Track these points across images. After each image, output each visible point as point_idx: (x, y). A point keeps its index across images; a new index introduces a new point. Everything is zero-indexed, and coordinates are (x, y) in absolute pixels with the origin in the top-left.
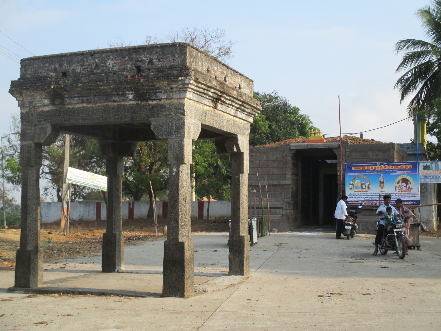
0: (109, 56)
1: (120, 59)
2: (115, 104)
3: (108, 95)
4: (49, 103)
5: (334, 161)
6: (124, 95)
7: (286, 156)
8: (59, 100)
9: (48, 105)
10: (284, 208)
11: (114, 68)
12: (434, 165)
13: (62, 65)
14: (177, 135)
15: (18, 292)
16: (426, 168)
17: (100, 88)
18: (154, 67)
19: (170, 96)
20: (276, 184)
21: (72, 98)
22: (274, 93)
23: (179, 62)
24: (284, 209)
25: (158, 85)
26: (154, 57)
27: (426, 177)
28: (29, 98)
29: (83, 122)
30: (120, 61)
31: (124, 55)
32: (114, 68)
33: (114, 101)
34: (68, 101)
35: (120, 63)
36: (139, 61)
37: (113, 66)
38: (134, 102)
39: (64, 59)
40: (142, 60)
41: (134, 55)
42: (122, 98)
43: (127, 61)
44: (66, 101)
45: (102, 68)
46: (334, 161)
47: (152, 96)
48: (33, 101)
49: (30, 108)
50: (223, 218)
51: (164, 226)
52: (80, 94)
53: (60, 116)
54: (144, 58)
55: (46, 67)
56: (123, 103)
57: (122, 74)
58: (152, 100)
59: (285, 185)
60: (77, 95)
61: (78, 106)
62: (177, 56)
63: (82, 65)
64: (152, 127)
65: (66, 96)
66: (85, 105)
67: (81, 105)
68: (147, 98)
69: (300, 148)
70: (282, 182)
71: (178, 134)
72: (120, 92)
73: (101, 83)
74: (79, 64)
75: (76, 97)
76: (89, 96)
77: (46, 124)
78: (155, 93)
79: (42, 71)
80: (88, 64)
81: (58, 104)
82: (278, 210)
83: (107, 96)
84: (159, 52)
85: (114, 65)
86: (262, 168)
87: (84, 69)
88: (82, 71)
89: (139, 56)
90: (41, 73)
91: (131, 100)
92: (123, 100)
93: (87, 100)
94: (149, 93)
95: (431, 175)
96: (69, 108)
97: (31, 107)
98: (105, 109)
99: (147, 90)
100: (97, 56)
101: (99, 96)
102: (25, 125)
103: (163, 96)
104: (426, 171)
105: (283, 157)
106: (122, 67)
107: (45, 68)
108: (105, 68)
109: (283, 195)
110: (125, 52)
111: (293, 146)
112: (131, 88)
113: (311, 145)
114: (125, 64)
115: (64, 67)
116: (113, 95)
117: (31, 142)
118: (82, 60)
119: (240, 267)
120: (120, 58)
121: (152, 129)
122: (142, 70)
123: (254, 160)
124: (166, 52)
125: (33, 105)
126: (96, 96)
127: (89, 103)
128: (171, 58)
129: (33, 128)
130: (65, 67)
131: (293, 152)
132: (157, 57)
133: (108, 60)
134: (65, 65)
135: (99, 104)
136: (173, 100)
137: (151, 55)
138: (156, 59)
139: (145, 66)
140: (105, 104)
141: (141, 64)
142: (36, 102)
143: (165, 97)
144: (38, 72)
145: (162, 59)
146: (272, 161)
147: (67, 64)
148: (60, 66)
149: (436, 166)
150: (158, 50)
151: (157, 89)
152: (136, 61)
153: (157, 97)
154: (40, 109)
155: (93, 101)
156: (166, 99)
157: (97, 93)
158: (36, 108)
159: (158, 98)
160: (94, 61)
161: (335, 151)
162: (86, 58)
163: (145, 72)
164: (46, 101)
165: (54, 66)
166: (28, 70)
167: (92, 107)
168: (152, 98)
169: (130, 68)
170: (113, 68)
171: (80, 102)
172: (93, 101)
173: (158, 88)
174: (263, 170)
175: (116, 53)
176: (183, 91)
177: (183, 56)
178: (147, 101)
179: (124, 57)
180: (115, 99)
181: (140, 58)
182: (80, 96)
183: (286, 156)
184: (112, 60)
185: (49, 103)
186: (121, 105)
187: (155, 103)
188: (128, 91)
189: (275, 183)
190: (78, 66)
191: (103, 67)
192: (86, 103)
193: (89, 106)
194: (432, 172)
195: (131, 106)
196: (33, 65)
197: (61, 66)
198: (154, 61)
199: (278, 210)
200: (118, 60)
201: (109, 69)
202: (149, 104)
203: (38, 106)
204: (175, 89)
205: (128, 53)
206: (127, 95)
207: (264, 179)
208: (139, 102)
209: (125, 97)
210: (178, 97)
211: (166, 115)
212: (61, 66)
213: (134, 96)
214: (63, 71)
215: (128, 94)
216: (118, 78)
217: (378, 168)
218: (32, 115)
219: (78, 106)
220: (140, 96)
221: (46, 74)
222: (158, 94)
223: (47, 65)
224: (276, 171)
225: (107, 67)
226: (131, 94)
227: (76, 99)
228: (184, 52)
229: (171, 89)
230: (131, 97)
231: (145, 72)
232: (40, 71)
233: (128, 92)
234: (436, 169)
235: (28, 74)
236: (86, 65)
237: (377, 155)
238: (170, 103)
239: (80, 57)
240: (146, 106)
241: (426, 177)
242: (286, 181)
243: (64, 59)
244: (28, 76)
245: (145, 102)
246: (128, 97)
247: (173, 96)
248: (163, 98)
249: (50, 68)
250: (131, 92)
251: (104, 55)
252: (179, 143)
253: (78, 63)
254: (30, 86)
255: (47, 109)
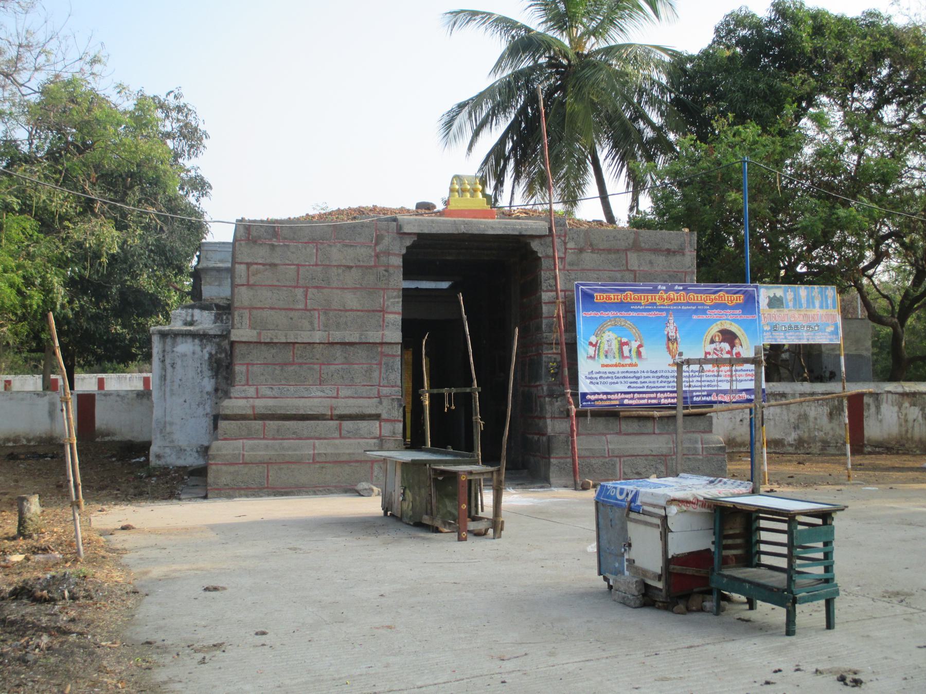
7: (388, 253)
10: (384, 416)
12: (790, 296)
16: (775, 303)
20: (352, 340)
22: (172, 95)
24: (387, 420)
59: (382, 344)
69: (434, 231)
70: (374, 336)
82: (363, 424)
104: (774, 311)
105: (377, 256)
109: (376, 374)
111: (409, 222)
123: (277, 261)
131: (408, 242)
146: (338, 266)
149: (795, 299)
161: (535, 245)
174: (310, 295)
183: (388, 253)
194: (788, 315)
207: (311, 323)
217: (661, 298)
224: (352, 301)
237: (651, 262)
241: (774, 328)
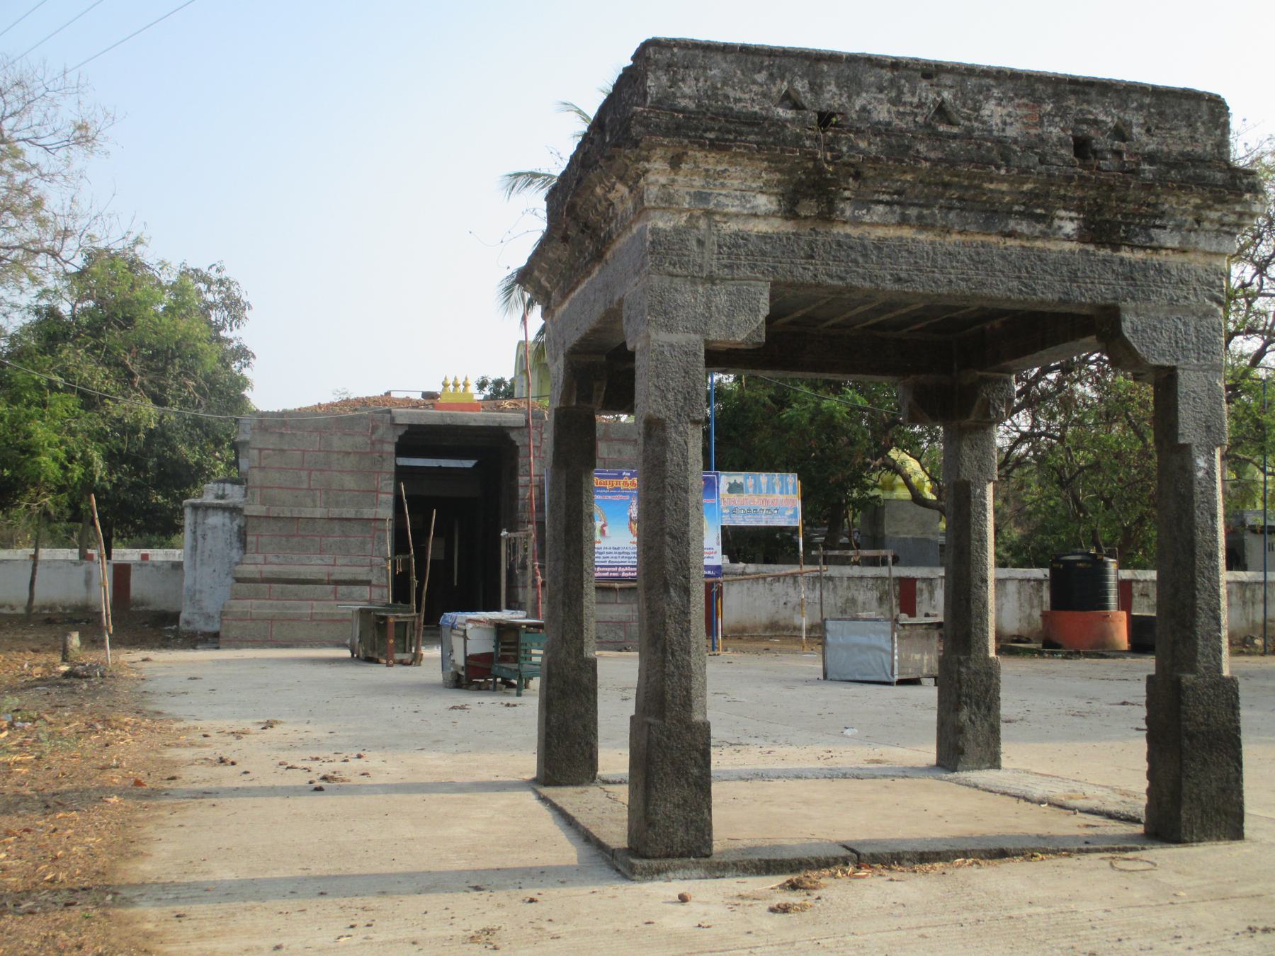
0: (989, 90)
1: (1026, 105)
2: (1010, 242)
3: (995, 212)
4: (774, 207)
5: (404, 462)
6: (1047, 219)
7: (382, 441)
8: (813, 203)
9: (767, 216)
10: (374, 582)
11: (1008, 128)
12: (750, 482)
13: (821, 87)
14: (1202, 362)
15: (680, 874)
16: (734, 488)
17: (986, 185)
18: (1134, 150)
19: (1188, 243)
20: (348, 516)
21: (865, 202)
22: (214, 268)
23: (1208, 148)
24: (376, 586)
25: (1166, 206)
26: (1136, 119)
27: (734, 511)
28: (698, 182)
29: (897, 287)
30: (1025, 111)
31: (1038, 94)
32: (1008, 128)
33: (1011, 234)
34: (848, 213)
35: (1026, 116)
36: (1086, 121)
37: (1005, 123)
38: (1074, 246)
39: (825, 68)
40: (1096, 122)
41: (1071, 102)
42: (1040, 227)
43: (1049, 114)
44: (843, 211)
45: (967, 123)
46: (404, 462)
47: (1137, 235)
48: (710, 194)
49: (691, 216)
50: (51, 609)
51: (66, 635)
52: (899, 193)
53: (812, 257)
54: (1102, 117)
55: (754, 82)
56: (1039, 244)
57: (1055, 154)
58: (1133, 247)
59: (375, 520)
60: (886, 198)
61: (880, 232)
62: (1202, 130)
63: (896, 101)
64: (1126, 327)
65: (847, 194)
66: (907, 233)
67: (892, 232)
68: (1122, 239)
69: (423, 423)
70: (368, 513)
71: (1204, 358)
72: (1038, 206)
73: (1003, 172)
74: (880, 96)
75: (879, 202)
76: (927, 206)
77: (757, 279)
78: (1146, 228)
79: (739, 94)
80: (916, 100)
81: (806, 218)
82: (356, 590)
83: (992, 214)
84: (1149, 105)
85: (1008, 120)
86: (310, 471)
87: (901, 115)
88: (896, 122)
89: (1085, 106)
90: (737, 100)
91: (1068, 238)
92: (1044, 236)
93: (920, 217)
94: (1128, 225)
95: (746, 506)
96: (848, 236)
97: (697, 213)
98: (978, 254)
99: (1125, 216)
100: (948, 80)
101: (962, 209)
102: (671, 275)
103: (1169, 239)
104: (733, 496)
105: (373, 443)
106: (1033, 131)
107: (755, 88)
108: (976, 124)
109: (369, 546)
110: (1040, 87)
111: (401, 415)
112: (1081, 199)
113: (451, 416)
114: (1041, 124)
115: (827, 96)
116: (1010, 213)
117: (698, 337)
118: (893, 82)
119: (989, 745)
120: (1025, 101)
121: (1127, 335)
122: (1095, 152)
123: (286, 447)
124: (1168, 111)
125: (711, 206)
126: (950, 208)
127: (923, 225)
128: (1184, 132)
129: (701, 289)
130: (832, 96)
131: (401, 432)
132: (1142, 121)
133: (987, 99)
134: (833, 88)
135: (955, 237)
136: (1192, 256)
137: (1124, 110)
138: (1142, 126)
139: (1102, 141)
140: (979, 238)
141: (1092, 133)
142: (721, 199)
143: (1176, 245)
144: (727, 97)
145: (1157, 128)
146: (338, 452)
147: (838, 86)
148: (812, 89)
149: (755, 485)
150: (1147, 100)
151: (1156, 217)
152: (1078, 122)
153: (1152, 240)
154: (733, 226)
155: (940, 223)
156: (1173, 250)
157: (960, 199)
158: (717, 218)
159: (1155, 244)
160: (939, 94)
161: (514, 435)
162: (908, 79)
163: (1105, 159)
164: (763, 202)
165: (791, 83)
166: (683, 80)
167: (932, 243)
168: (1136, 241)
169: (1060, 139)
170: (1004, 130)
171: (893, 219)
172: (940, 223)
173: (1162, 215)
174: (313, 477)
175: (1010, 85)
176: (1228, 233)
177: (1218, 132)
178: (1116, 247)
179: (1039, 101)
180: (1018, 228)
181: (1091, 113)
182: (900, 199)
183: (382, 441)
184: (999, 105)
185: (774, 207)
186: (1032, 249)
187: (1139, 255)
188: (1065, 209)
189: (349, 512)
190: (880, 101)
191: (969, 120)
192: (911, 226)
193: (921, 237)
194: (746, 500)
195: (1065, 259)
196: (705, 68)
197: (816, 88)
198: (1135, 130)
199: (358, 588)
200: (1019, 106)
201: (991, 131)
202: (1122, 260)
203: (725, 215)
204: (1206, 225)
205: (1050, 91)
206: (1057, 222)
207: (314, 501)
208: (1091, 248)
209: (1050, 226)
210: (1214, 248)
211: (1172, 299)
212: (816, 88)
213: (1080, 229)
214: (824, 108)
215: (1062, 219)
216: (1042, 162)
217: (625, 483)
218: (700, 243)
219: (880, 232)
220: (1099, 231)
221: (757, 109)
222: (1154, 232)
223: (761, 77)
224: (350, 482)
225: (984, 123)
226: (1071, 219)
227: (881, 208)
228: (1222, 120)
229: (1198, 221)
230: (1069, 227)
231: (1105, 159)
232: (731, 93)
233: (1063, 213)
234: (754, 492)
235: (684, 96)
236: (911, 104)
237: (619, 451)
238: (1183, 264)
239: (887, 74)
240: (1112, 262)
241: (734, 511)
242: (380, 510)
243: (825, 68)
244: (683, 103)
245: (1109, 251)
246: (1060, 228)
247: (1197, 243)
248: (1169, 245)
249: (774, 90)
250: (1073, 214)
251: (971, 83)
252: (1210, 384)
253: (881, 92)
254: (735, 140)
255: (762, 227)
